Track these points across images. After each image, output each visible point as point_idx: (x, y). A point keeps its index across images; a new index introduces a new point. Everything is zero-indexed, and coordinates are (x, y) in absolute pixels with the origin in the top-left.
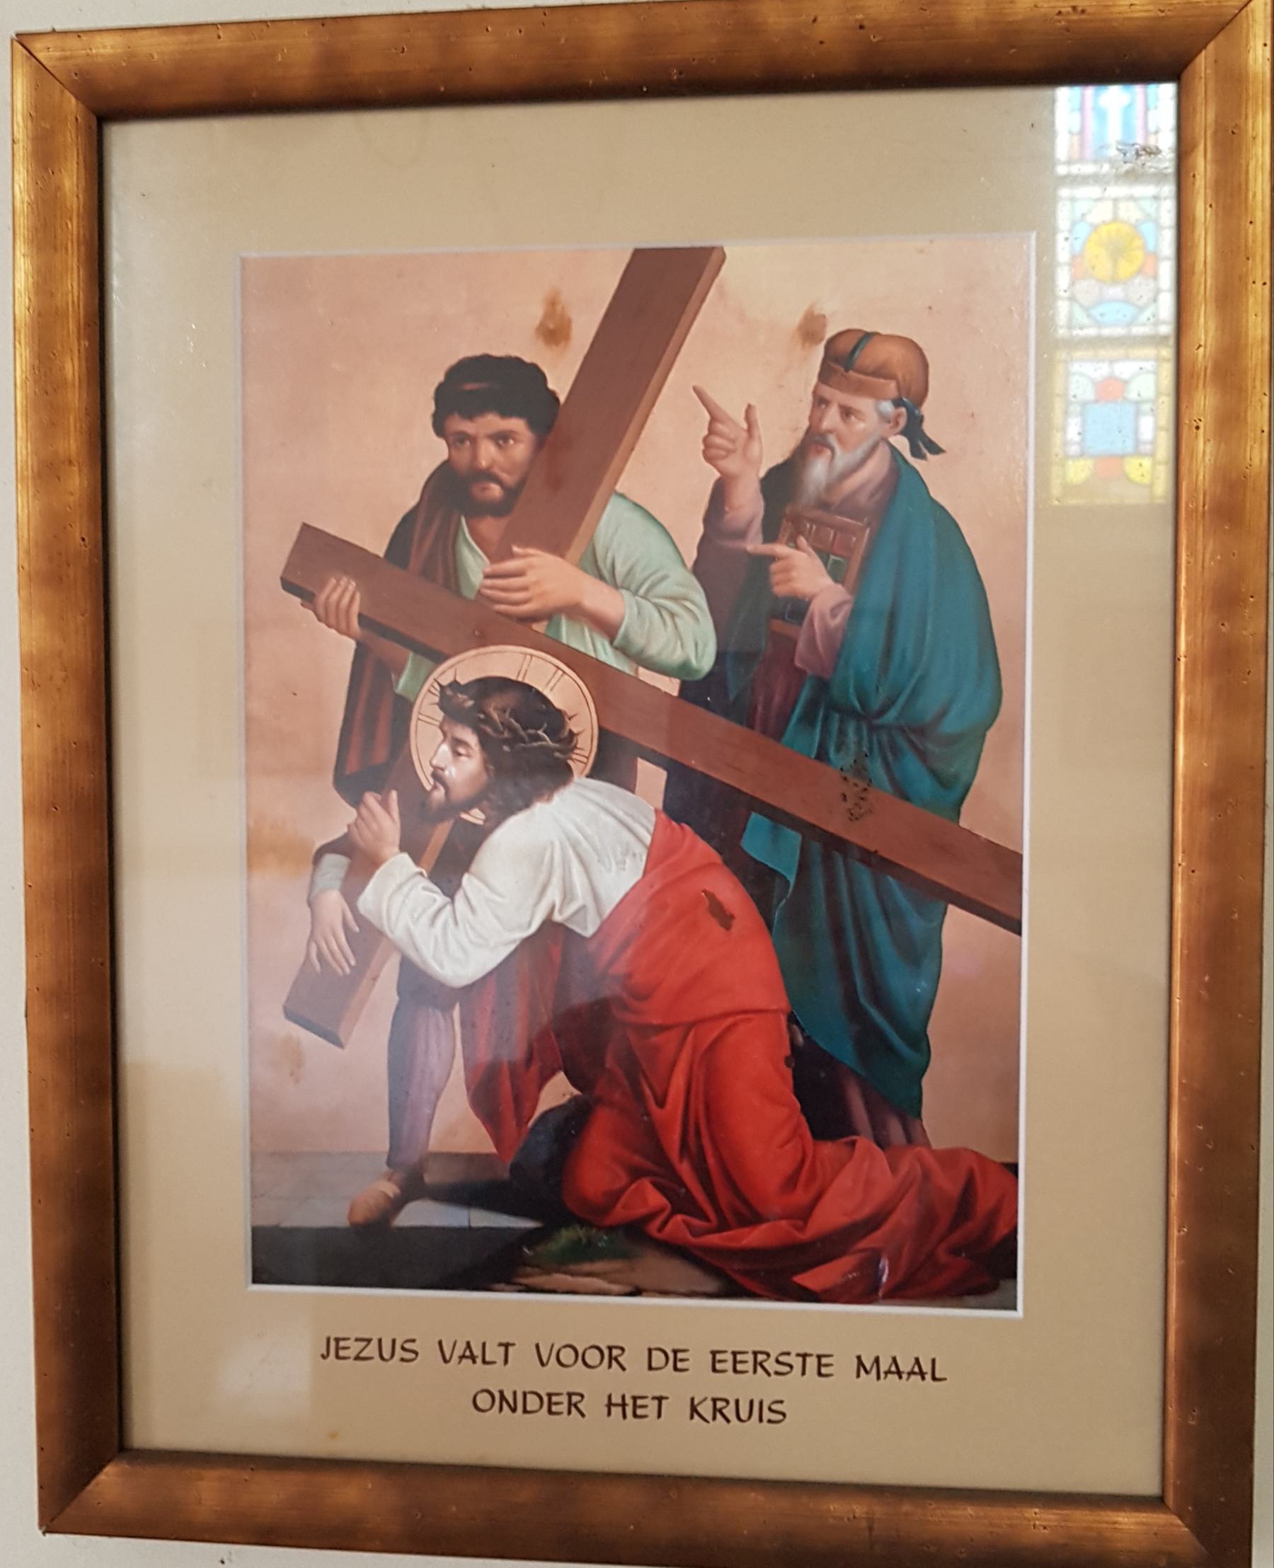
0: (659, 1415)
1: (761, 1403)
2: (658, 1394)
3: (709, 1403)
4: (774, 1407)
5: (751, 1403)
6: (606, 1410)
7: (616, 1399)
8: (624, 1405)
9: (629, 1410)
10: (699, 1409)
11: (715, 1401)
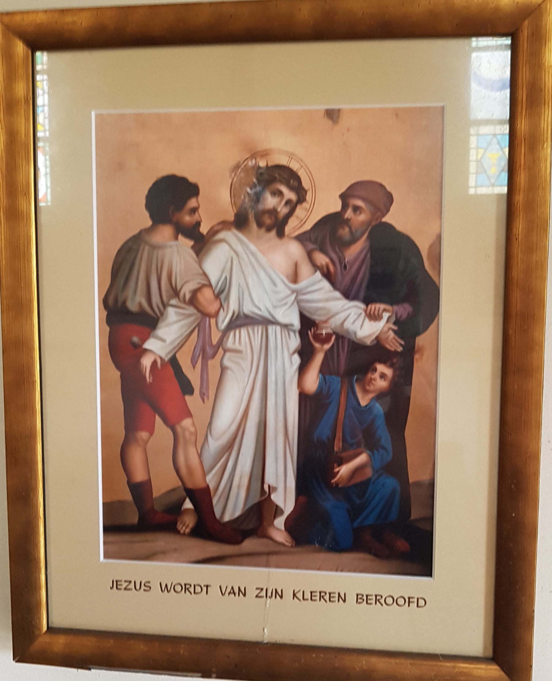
10: (297, 595)
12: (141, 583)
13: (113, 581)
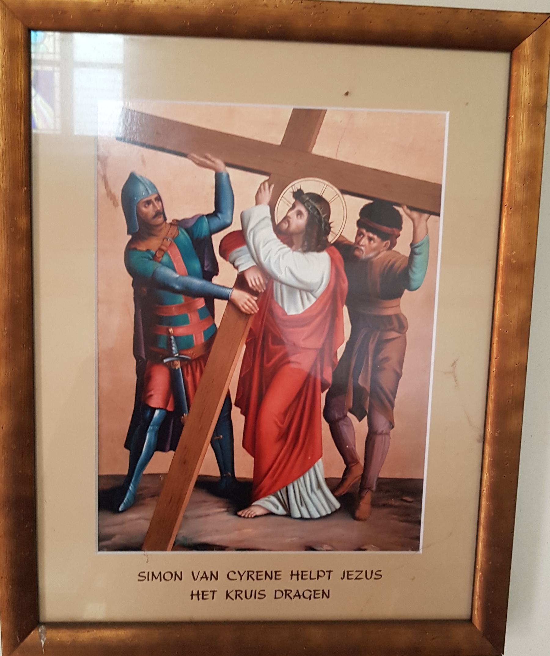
0: (213, 598)
1: (256, 591)
2: (213, 590)
3: (234, 593)
4: (261, 593)
5: (252, 591)
6: (191, 597)
7: (195, 592)
8: (198, 595)
9: (201, 597)
10: (230, 595)
11: (236, 591)
12: (372, 571)
13: (344, 572)
